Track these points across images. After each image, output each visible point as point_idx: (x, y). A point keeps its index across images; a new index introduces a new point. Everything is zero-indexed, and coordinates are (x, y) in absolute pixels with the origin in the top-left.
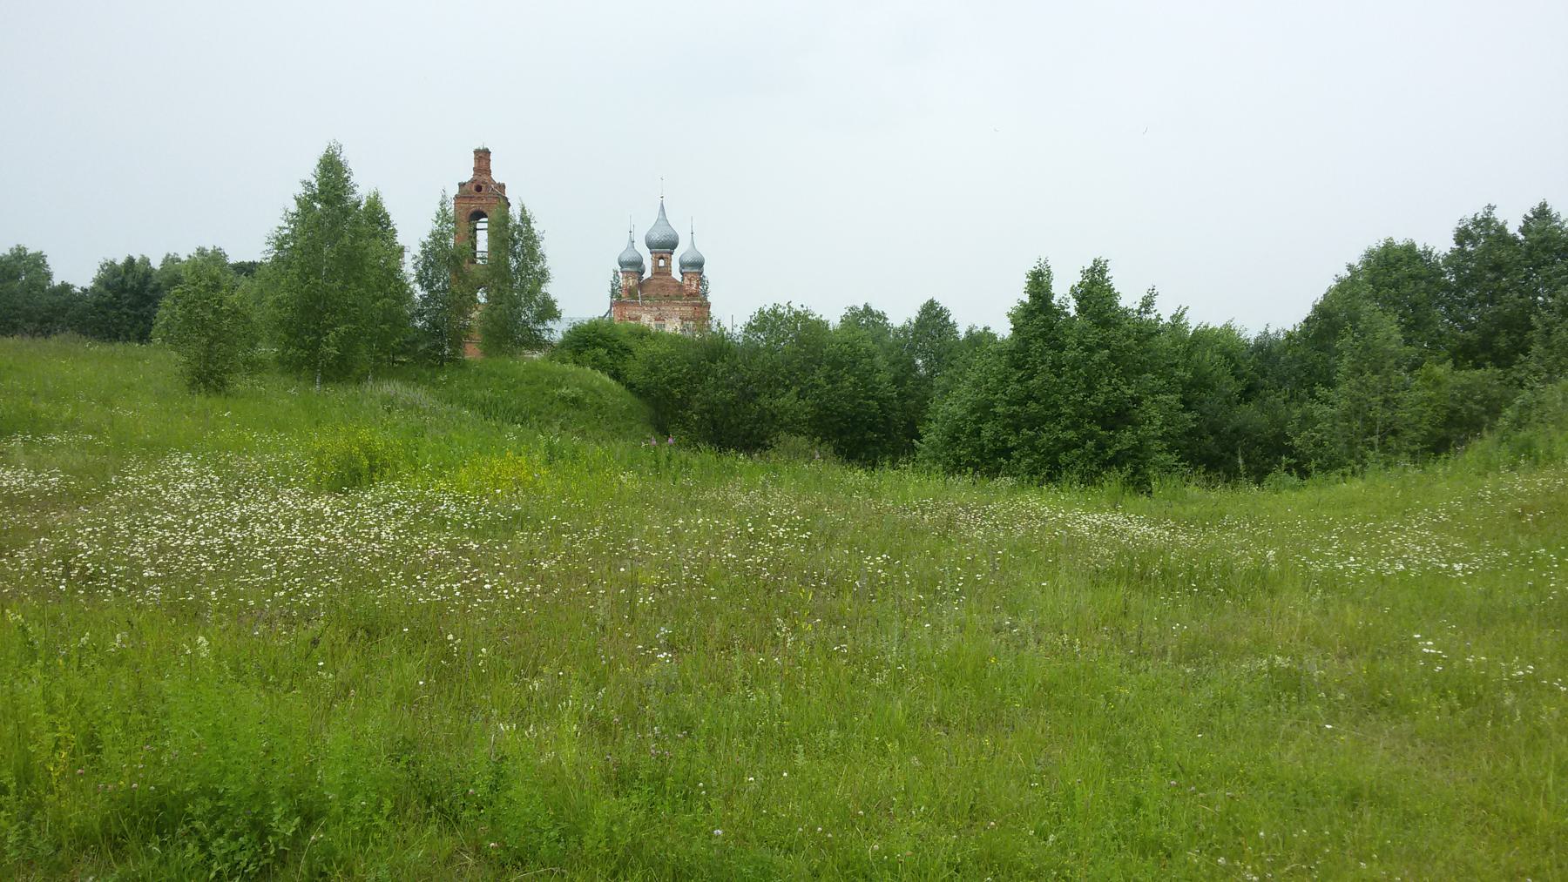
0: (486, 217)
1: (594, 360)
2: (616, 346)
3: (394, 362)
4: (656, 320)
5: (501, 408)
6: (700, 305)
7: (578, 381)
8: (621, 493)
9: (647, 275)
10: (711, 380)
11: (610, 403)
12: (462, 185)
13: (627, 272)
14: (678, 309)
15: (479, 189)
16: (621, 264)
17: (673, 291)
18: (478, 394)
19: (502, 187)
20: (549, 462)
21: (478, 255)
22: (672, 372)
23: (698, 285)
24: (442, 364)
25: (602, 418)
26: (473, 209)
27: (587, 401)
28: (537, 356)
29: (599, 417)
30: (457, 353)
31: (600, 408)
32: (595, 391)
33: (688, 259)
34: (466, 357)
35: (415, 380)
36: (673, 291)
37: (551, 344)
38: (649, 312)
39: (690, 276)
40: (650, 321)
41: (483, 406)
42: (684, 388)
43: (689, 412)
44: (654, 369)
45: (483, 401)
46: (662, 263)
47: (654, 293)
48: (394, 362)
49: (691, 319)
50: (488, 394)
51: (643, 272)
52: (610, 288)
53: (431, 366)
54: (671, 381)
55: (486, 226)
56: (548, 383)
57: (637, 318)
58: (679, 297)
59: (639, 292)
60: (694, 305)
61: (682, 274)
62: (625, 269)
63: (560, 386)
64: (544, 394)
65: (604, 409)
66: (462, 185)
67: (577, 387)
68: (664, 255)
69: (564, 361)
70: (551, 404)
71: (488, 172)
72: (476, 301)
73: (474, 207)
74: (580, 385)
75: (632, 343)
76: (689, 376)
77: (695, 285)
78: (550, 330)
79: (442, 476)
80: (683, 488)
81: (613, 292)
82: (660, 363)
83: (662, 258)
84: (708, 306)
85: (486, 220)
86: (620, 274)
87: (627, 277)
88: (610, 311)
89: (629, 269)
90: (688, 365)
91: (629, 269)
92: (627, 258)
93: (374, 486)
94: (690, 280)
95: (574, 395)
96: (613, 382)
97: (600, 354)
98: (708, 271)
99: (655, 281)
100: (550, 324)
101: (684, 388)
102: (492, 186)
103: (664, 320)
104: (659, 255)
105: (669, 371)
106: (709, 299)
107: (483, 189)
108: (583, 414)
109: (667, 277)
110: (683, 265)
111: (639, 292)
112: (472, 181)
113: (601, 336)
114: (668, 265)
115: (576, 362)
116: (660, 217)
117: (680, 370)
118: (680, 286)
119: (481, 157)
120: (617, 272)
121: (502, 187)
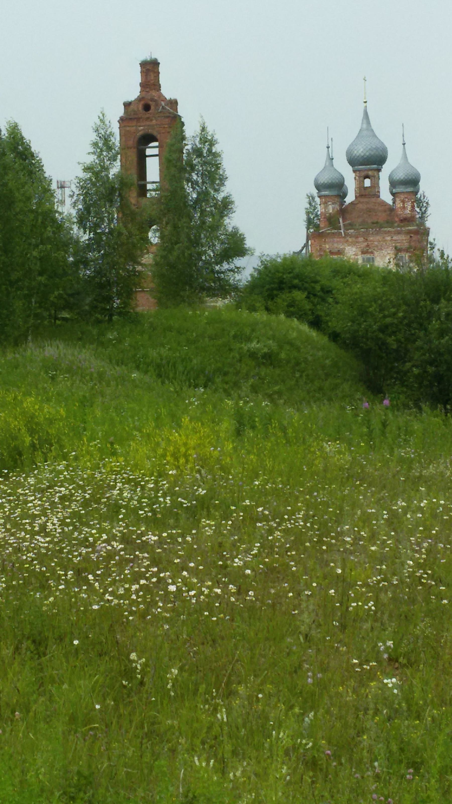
0: (156, 140)
1: (290, 306)
2: (318, 287)
3: (56, 318)
4: (363, 253)
5: (180, 368)
6: (416, 232)
7: (271, 333)
8: (325, 470)
9: (350, 198)
10: (435, 324)
11: (310, 358)
12: (127, 105)
13: (325, 196)
14: (389, 238)
15: (147, 108)
16: (319, 187)
17: (382, 217)
18: (153, 353)
19: (174, 103)
20: (239, 433)
21: (149, 187)
22: (385, 317)
23: (413, 207)
24: (110, 320)
25: (301, 376)
26: (141, 133)
27: (283, 355)
28: (220, 303)
29: (297, 375)
30: (126, 304)
31: (298, 364)
32: (291, 344)
33: (400, 175)
34: (139, 309)
35: (80, 339)
36: (382, 217)
37: (236, 288)
38: (353, 244)
39: (402, 197)
40: (356, 255)
41: (159, 366)
42: (400, 336)
43: (408, 365)
44: (363, 312)
45: (159, 361)
46: (367, 183)
47: (360, 220)
48: (56, 318)
49: (407, 250)
50: (164, 352)
51: (345, 195)
52: (305, 217)
53: (99, 322)
54: (384, 329)
55: (156, 151)
56: (235, 337)
57: (340, 252)
58: (390, 223)
59: (341, 220)
60: (409, 232)
61: (393, 194)
62: (323, 193)
63: (249, 339)
64: (231, 350)
65: (303, 365)
66: (127, 105)
67: (269, 339)
68: (370, 173)
69: (252, 309)
70: (240, 361)
71: (157, 87)
72: (146, 240)
73: (141, 130)
74: (273, 338)
75: (337, 283)
76: (406, 321)
77: (409, 208)
78: (238, 270)
79: (114, 453)
80: (401, 460)
81: (310, 222)
82: (371, 306)
83: (367, 177)
84: (427, 232)
85: (156, 144)
86: (318, 200)
87: (325, 203)
88: (306, 245)
89: (326, 193)
90: (404, 307)
91: (326, 193)
92: (325, 179)
93: (37, 468)
94: (403, 202)
95: (266, 350)
96: (314, 334)
97: (299, 298)
98: (423, 187)
99: (360, 206)
100: (239, 262)
101: (400, 336)
102: (163, 103)
103: (372, 253)
104: (363, 174)
105: (381, 315)
106: (428, 224)
107: (152, 107)
108: (278, 371)
109: (373, 200)
110: (393, 184)
111: (341, 220)
112: (139, 99)
113: (297, 276)
114: (375, 185)
115: (267, 309)
116: (365, 126)
117: (395, 314)
118: (391, 210)
119: (148, 70)
120: (313, 198)
121: (174, 103)
